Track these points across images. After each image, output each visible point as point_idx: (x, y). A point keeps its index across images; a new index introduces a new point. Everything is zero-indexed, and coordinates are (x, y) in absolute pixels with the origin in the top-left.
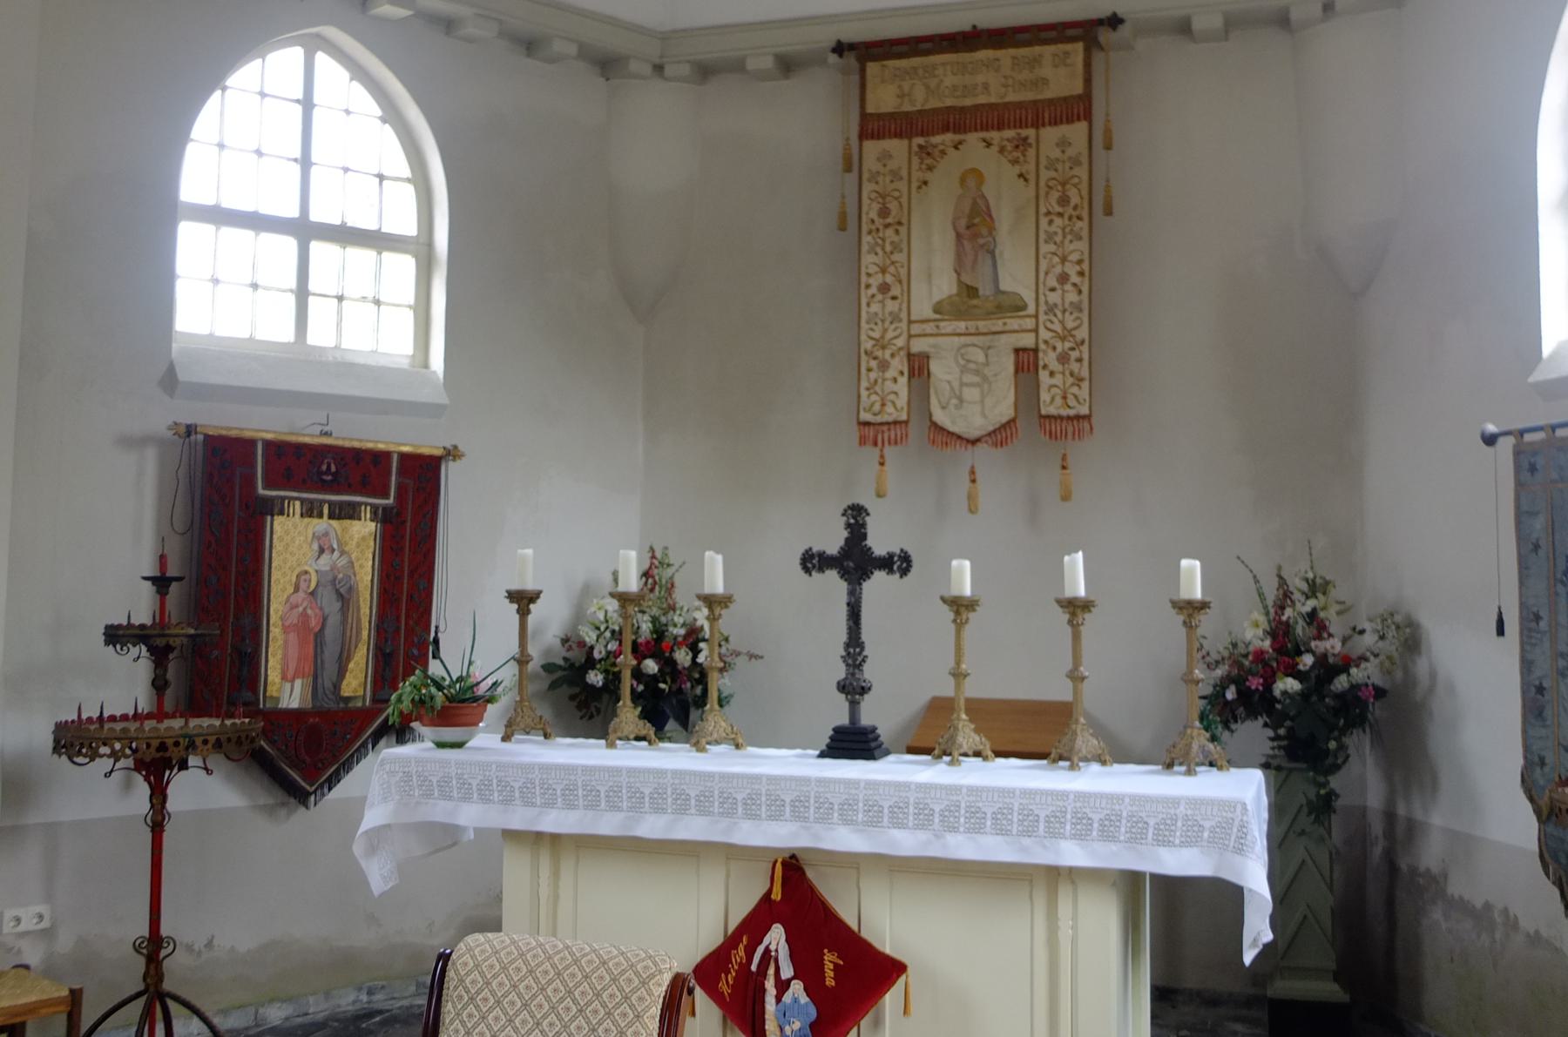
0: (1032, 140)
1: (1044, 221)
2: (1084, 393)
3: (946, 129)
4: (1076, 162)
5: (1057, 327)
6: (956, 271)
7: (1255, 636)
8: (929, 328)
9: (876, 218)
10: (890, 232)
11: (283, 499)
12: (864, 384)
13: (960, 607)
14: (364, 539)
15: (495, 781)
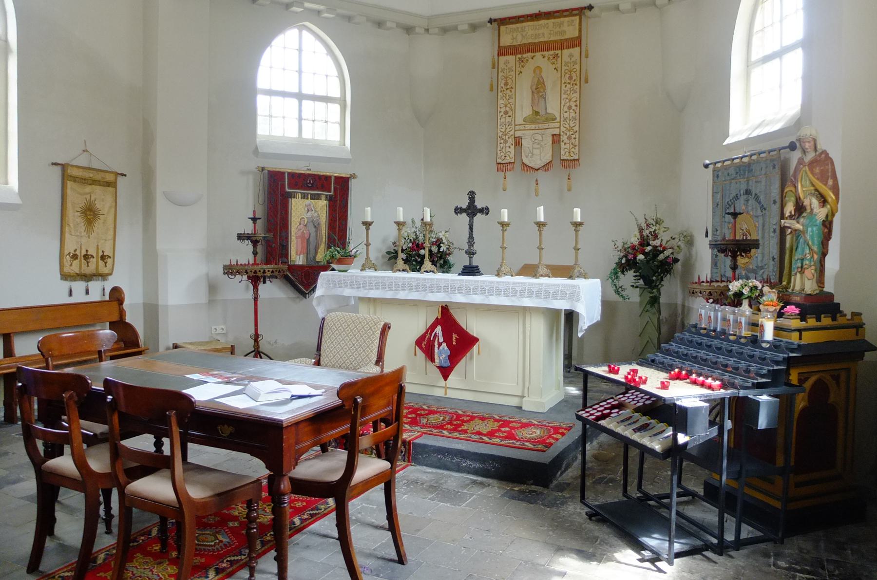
0: (559, 55)
1: (563, 86)
2: (577, 151)
4: (575, 63)
5: (567, 126)
7: (635, 240)
8: (522, 127)
10: (508, 91)
11: (295, 192)
12: (499, 149)
13: (503, 225)
14: (323, 206)
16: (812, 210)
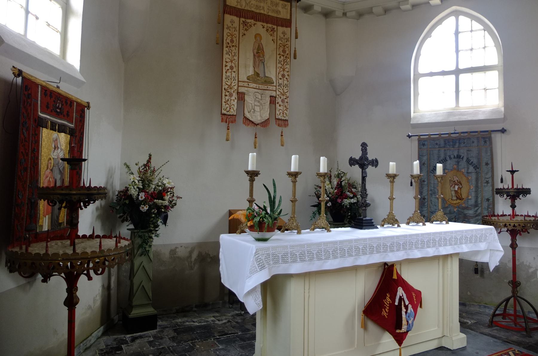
0: (275, 29)
3: (252, 18)
5: (282, 91)
6: (253, 67)
8: (246, 85)
9: (230, 43)
10: (233, 48)
12: (224, 100)
13: (392, 177)
15: (306, 252)
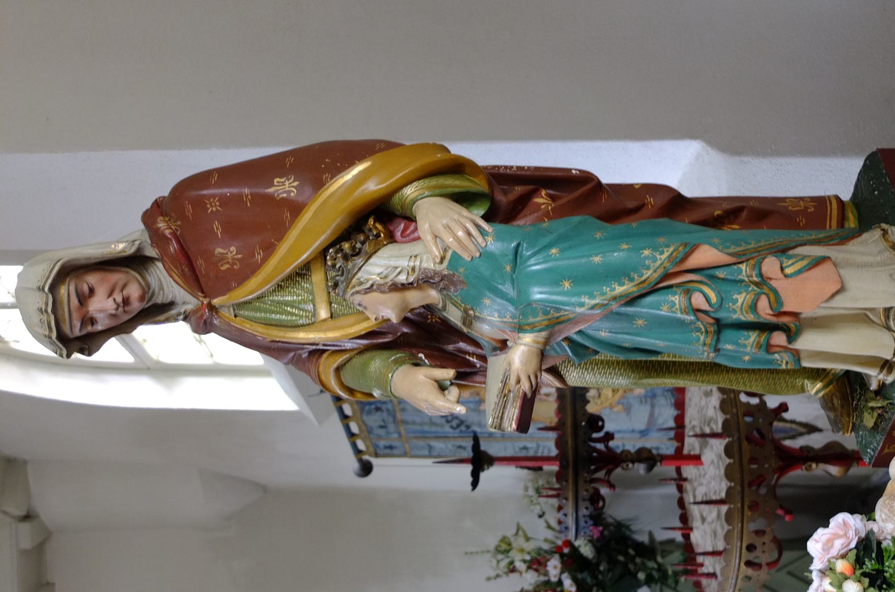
16: (425, 281)
